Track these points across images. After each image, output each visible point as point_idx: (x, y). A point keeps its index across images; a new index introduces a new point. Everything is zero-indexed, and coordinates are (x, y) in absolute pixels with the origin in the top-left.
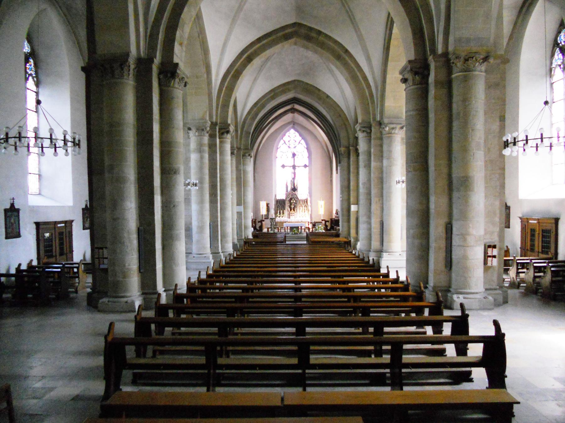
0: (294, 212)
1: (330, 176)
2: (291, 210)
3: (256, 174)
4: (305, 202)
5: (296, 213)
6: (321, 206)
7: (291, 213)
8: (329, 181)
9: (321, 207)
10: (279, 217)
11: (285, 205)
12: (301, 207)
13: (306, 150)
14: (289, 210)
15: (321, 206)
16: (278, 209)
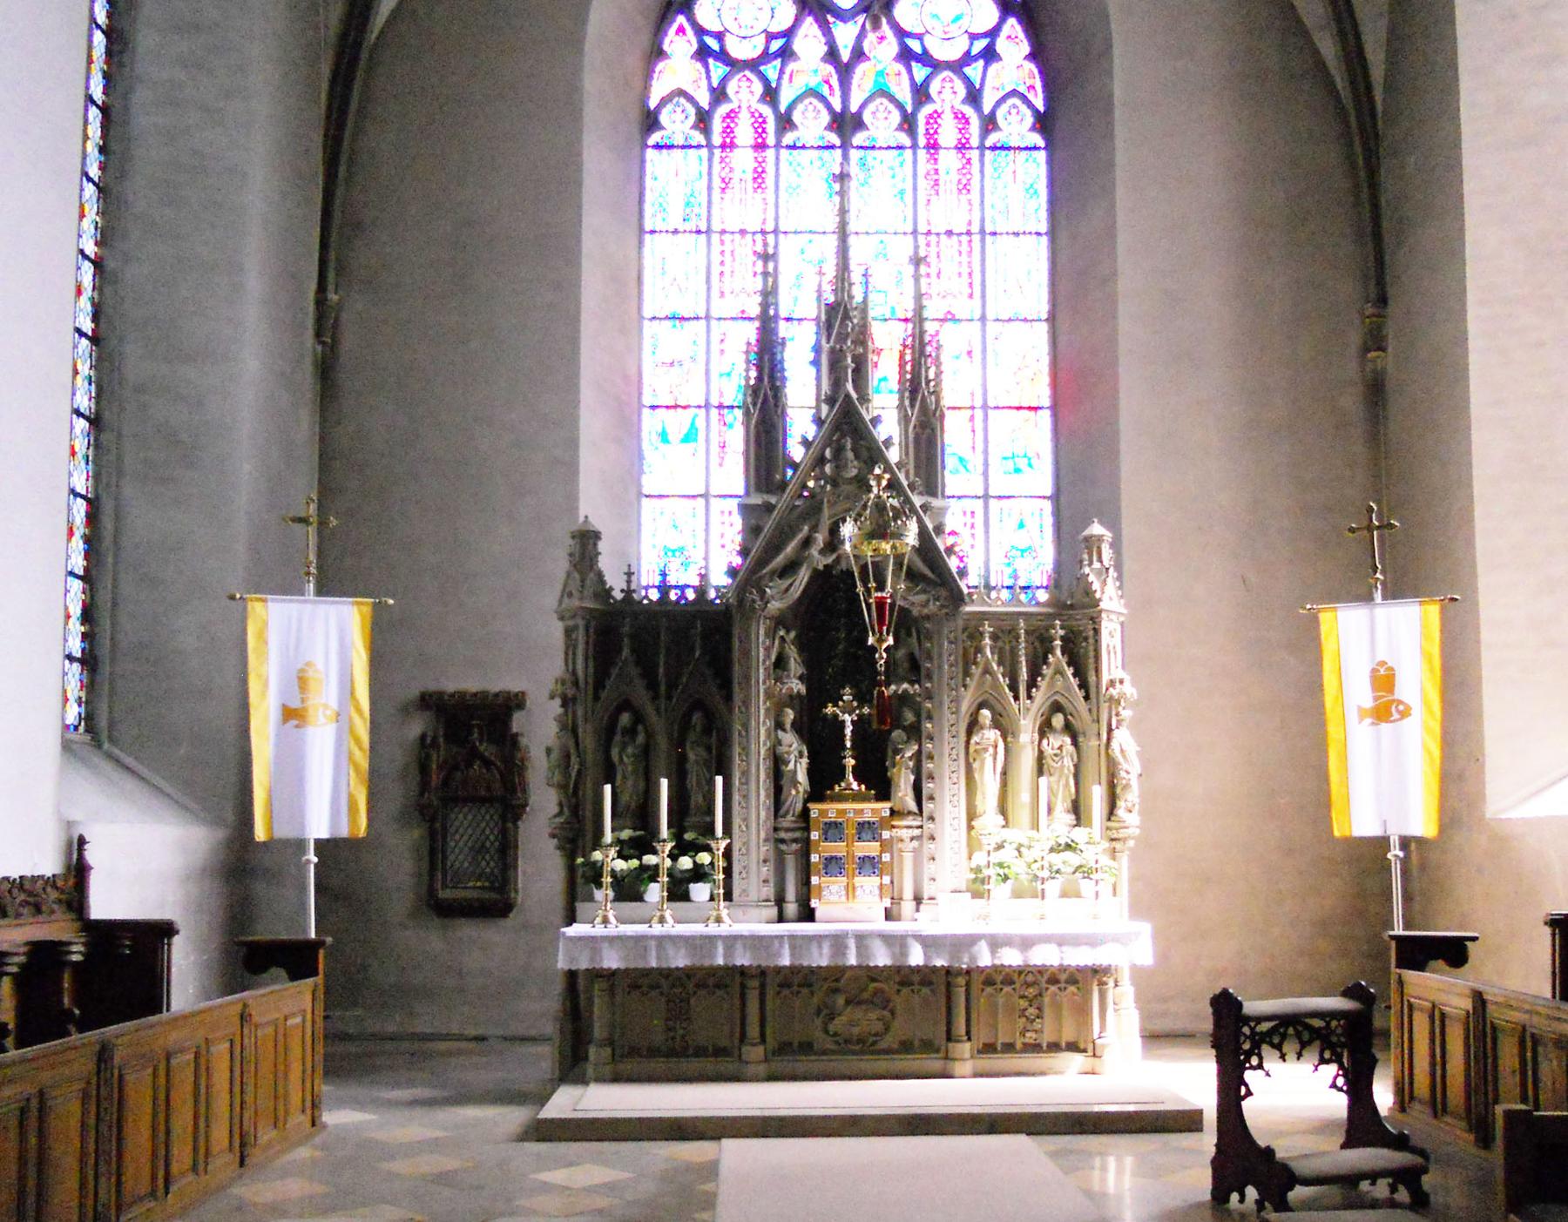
0: (873, 810)
1: (1355, 338)
2: (823, 781)
3: (354, 308)
4: (1057, 657)
5: (904, 831)
6: (1384, 680)
7: (833, 830)
8: (1351, 402)
9: (1386, 709)
10: (678, 891)
11: (726, 686)
12: (991, 735)
13: (1014, 45)
14: (799, 769)
15: (1384, 680)
16: (625, 757)
